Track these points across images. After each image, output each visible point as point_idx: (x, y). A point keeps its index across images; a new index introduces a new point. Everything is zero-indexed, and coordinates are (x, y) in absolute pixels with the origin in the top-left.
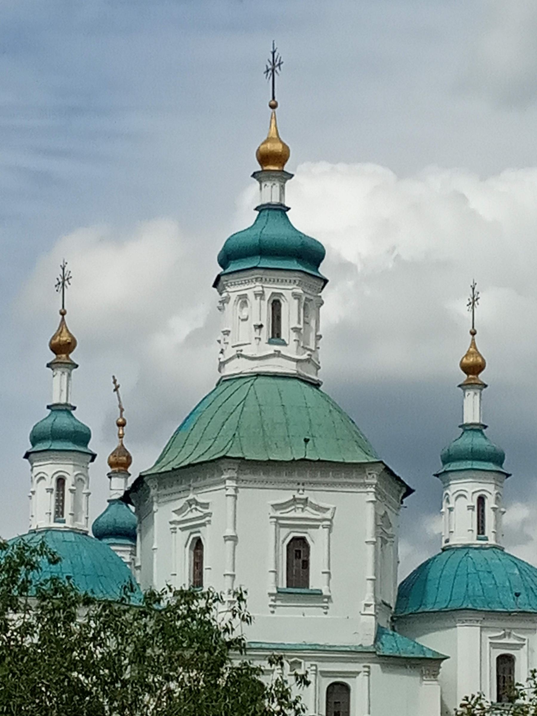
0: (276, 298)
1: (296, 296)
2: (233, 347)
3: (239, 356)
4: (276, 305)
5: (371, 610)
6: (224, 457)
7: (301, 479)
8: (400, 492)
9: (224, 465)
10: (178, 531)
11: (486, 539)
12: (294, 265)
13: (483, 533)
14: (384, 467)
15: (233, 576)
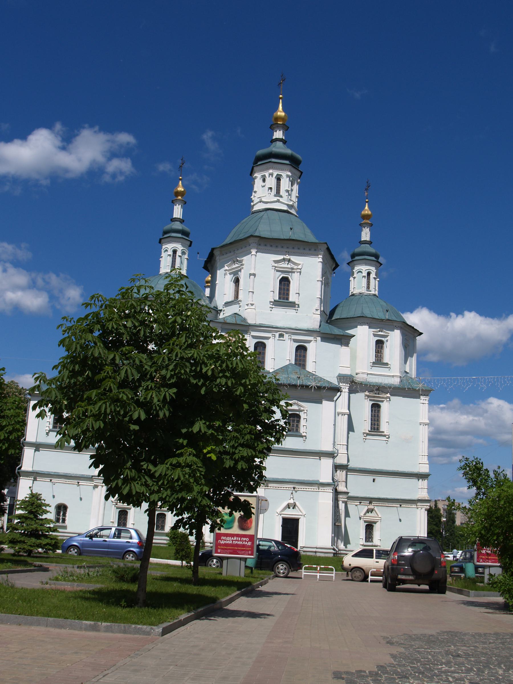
0: (279, 177)
1: (288, 176)
2: (258, 198)
3: (260, 202)
4: (278, 179)
5: (319, 312)
6: (252, 236)
7: (287, 250)
8: (332, 265)
9: (251, 240)
10: (228, 274)
11: (371, 291)
12: (287, 162)
13: (369, 289)
14: (327, 247)
15: (253, 292)
